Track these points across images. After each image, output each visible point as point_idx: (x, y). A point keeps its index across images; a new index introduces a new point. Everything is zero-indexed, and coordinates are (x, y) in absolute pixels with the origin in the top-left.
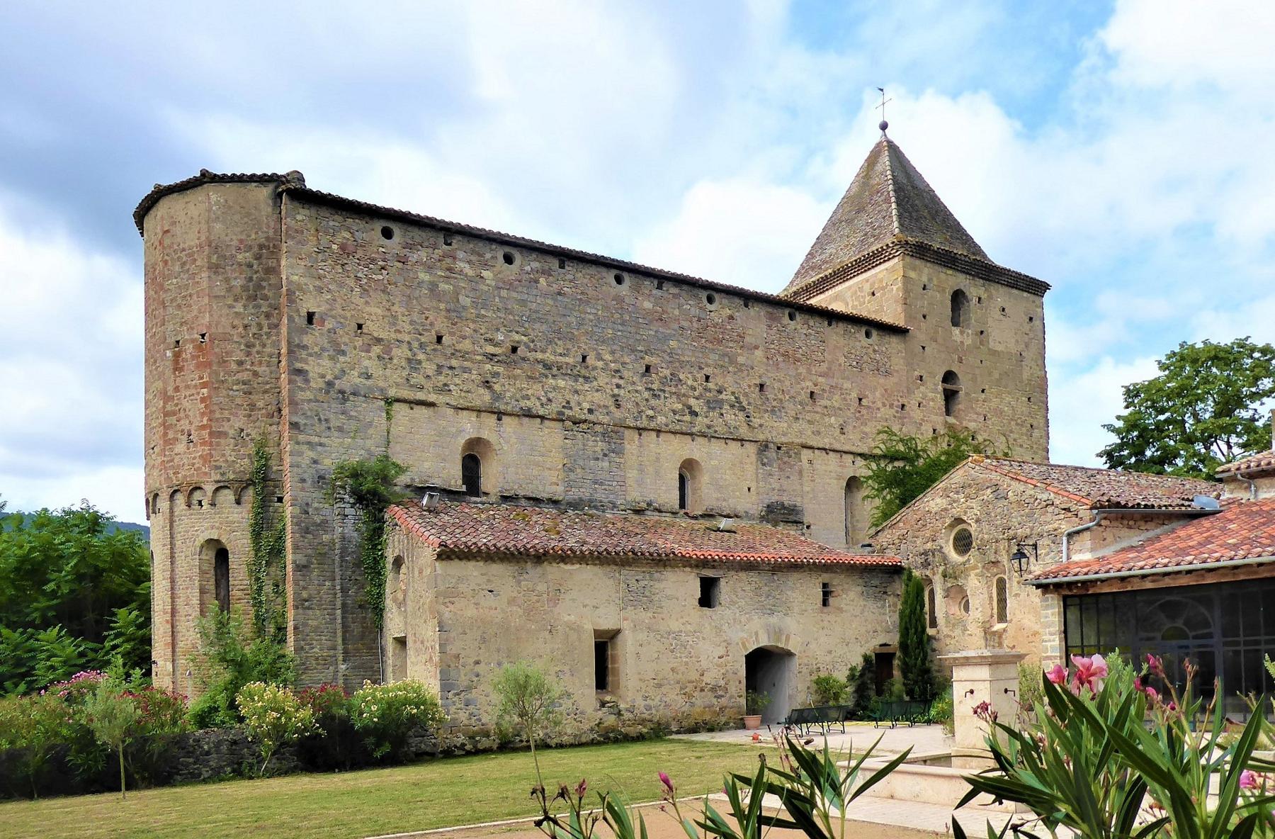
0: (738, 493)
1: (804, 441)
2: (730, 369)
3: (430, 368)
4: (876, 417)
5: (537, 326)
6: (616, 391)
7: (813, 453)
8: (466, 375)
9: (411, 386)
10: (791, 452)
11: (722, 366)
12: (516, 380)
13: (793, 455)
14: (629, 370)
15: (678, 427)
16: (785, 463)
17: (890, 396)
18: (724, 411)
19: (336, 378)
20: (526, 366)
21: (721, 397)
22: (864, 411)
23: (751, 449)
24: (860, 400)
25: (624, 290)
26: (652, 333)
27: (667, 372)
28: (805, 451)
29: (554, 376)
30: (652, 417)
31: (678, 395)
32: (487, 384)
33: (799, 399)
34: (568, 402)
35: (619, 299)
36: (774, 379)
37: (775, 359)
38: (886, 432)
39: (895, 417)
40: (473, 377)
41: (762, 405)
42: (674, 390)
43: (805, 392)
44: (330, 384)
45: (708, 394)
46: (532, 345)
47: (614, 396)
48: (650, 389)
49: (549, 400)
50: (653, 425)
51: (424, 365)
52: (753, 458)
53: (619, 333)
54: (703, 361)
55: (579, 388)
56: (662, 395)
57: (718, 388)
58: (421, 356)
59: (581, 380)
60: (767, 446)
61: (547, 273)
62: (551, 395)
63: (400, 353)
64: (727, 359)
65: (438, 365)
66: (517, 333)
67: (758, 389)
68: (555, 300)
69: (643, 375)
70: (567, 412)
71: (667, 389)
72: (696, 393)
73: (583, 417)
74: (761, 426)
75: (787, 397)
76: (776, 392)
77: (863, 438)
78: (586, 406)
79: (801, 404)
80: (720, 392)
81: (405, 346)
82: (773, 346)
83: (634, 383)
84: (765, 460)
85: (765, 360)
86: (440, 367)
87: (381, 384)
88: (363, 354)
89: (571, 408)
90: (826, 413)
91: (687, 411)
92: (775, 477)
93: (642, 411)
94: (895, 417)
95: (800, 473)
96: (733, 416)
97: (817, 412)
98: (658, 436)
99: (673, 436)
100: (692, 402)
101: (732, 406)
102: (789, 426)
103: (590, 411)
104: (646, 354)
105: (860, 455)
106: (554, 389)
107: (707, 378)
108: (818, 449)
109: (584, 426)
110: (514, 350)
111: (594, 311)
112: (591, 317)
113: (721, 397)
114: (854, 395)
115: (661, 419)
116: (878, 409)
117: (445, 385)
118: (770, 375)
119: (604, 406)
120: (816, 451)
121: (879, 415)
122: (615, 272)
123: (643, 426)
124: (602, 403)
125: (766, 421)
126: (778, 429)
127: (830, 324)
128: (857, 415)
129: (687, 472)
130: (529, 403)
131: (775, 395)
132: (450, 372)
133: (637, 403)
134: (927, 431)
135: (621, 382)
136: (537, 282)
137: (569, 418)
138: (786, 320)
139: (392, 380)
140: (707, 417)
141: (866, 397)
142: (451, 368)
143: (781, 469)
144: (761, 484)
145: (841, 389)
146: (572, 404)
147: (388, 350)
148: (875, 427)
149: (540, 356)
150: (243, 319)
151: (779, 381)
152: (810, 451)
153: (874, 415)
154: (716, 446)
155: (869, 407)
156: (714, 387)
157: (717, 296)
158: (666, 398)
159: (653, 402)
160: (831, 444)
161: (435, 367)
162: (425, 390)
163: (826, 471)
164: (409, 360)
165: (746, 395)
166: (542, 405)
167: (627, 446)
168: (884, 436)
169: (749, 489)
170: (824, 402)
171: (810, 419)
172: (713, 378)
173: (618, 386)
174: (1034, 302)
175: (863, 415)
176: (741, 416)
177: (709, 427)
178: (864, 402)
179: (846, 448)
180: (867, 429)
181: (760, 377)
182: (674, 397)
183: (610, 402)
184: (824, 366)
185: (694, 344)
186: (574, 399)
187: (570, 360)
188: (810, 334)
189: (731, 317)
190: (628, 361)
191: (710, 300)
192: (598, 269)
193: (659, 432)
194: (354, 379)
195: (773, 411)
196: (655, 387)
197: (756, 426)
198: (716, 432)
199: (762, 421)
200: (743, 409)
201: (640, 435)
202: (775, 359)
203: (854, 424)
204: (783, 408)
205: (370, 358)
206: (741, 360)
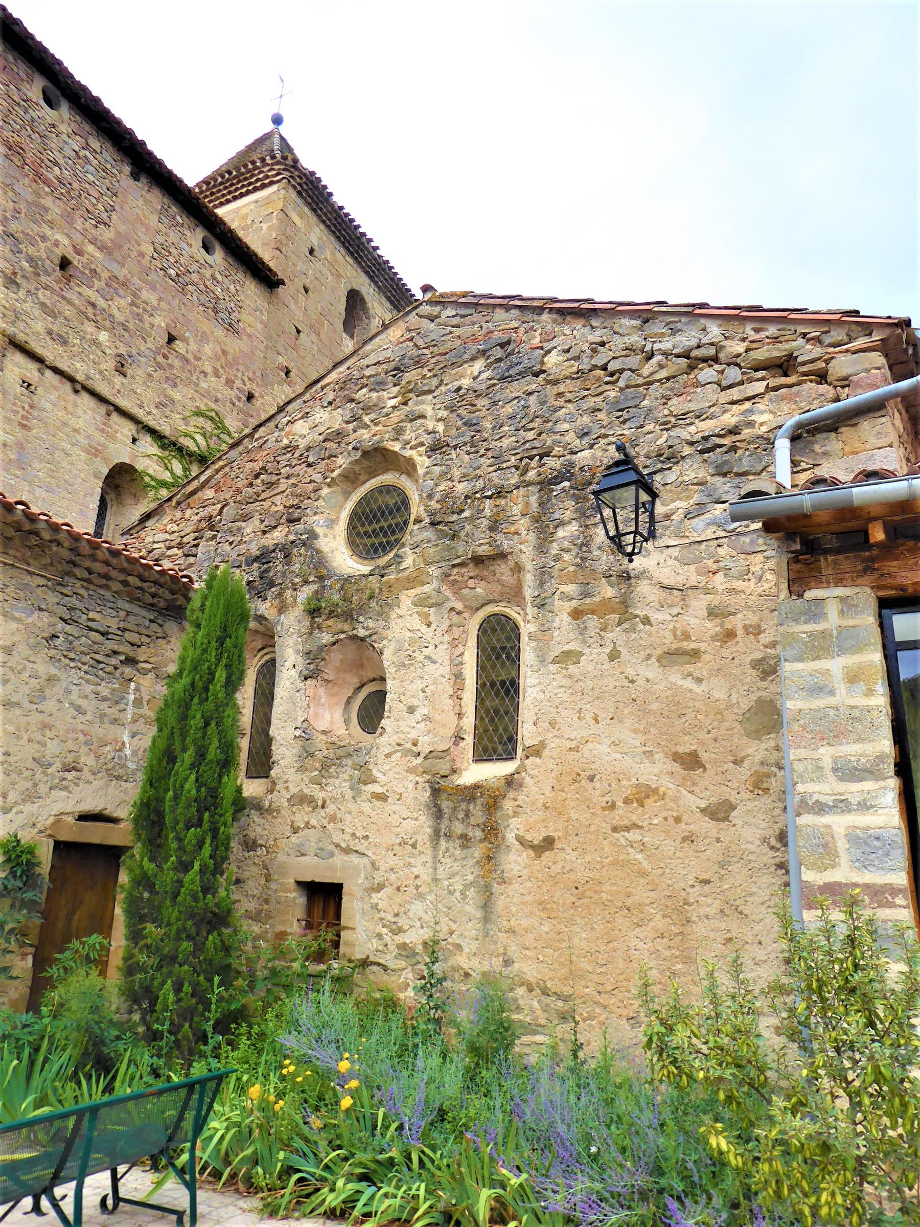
1: (21, 337)
4: (197, 385)
17: (229, 365)
24: (171, 339)
38: (211, 419)
79: (31, 260)
97: (70, 303)
105: (152, 432)
108: (56, 370)
114: (160, 321)
116: (205, 374)
120: (48, 373)
121: (203, 385)
128: (160, 359)
141: (185, 340)
145: (135, 295)
152: (33, 366)
153: (194, 379)
160: (88, 377)
163: (65, 424)
168: (209, 426)
171: (48, 302)
175: (171, 366)
180: (176, 395)
184: (106, 235)
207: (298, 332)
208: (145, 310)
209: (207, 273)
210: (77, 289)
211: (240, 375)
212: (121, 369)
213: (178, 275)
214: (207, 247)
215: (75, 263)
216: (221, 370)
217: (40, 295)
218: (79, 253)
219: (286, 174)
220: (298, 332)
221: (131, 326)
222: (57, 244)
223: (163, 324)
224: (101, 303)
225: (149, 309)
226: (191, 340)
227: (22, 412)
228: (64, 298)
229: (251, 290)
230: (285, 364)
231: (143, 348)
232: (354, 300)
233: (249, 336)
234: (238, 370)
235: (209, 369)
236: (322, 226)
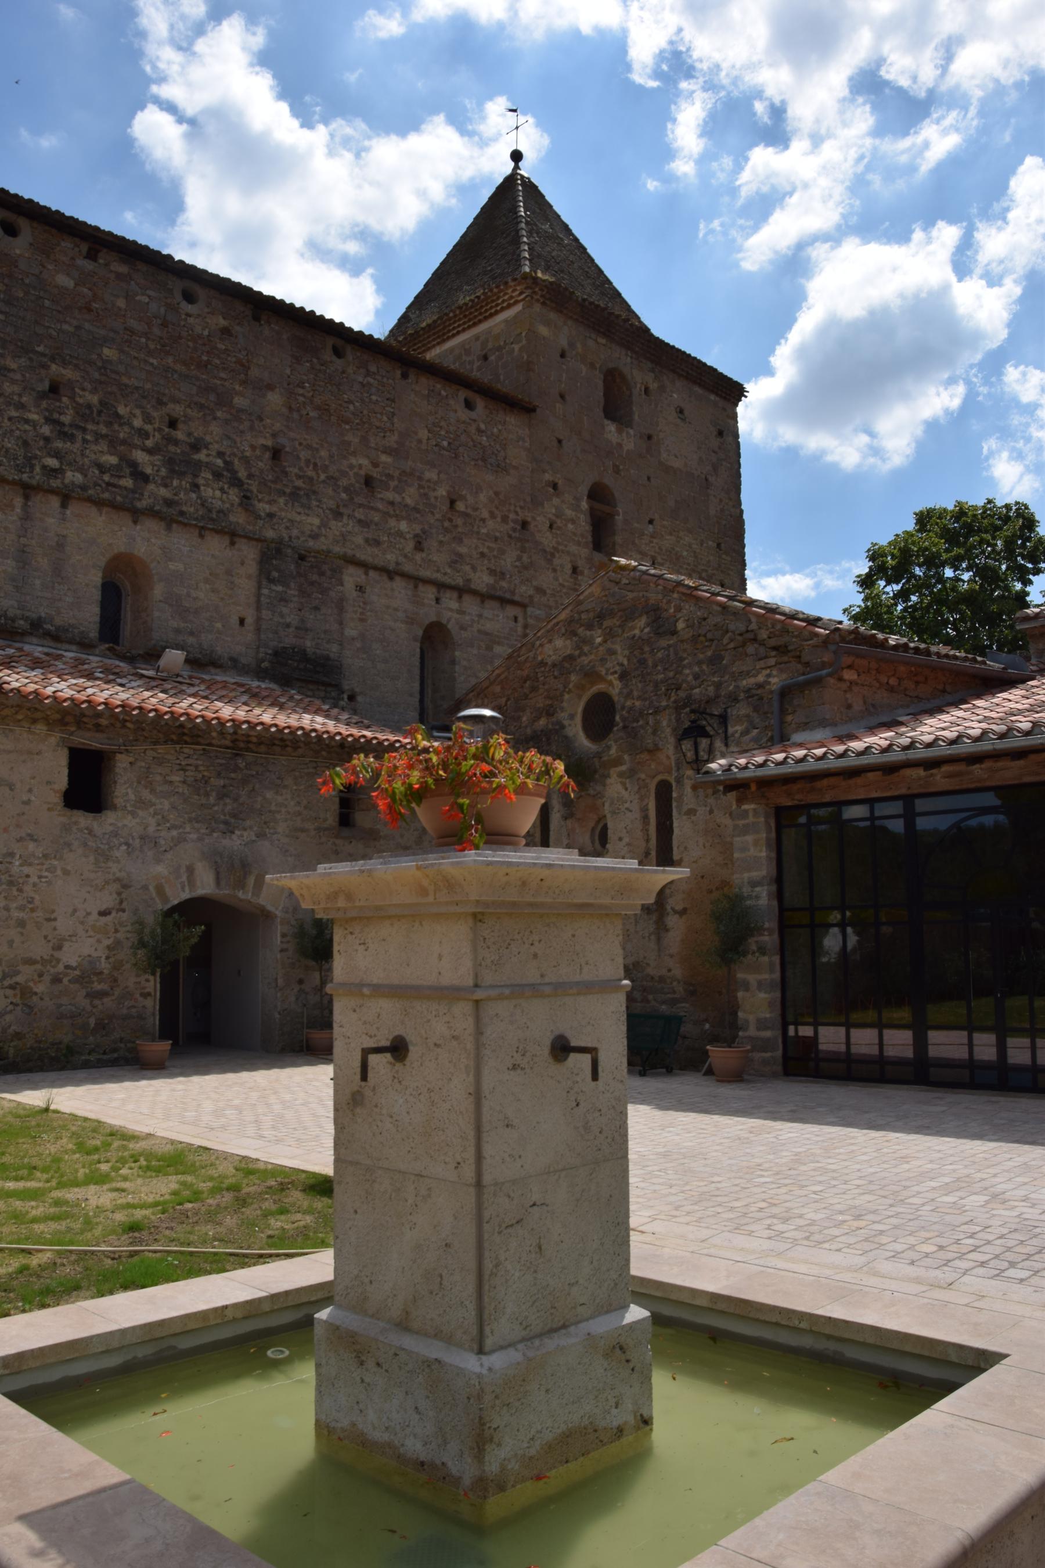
0: (219, 625)
1: (350, 552)
2: (219, 414)
4: (478, 533)
7: (366, 574)
10: (325, 567)
11: (202, 407)
13: (329, 573)
14: (13, 382)
15: (106, 495)
16: (312, 583)
18: (201, 481)
21: (196, 457)
22: (459, 521)
23: (250, 553)
24: (452, 502)
27: (94, 399)
28: (351, 570)
31: (113, 443)
33: (344, 482)
36: (300, 444)
37: (304, 412)
39: (510, 536)
41: (274, 482)
42: (104, 430)
43: (356, 474)
45: (172, 448)
48: (57, 422)
50: (55, 483)
52: (252, 568)
54: (167, 391)
56: (79, 436)
60: (279, 551)
64: (212, 397)
67: (268, 455)
69: (42, 396)
72: (149, 443)
74: (271, 515)
75: (323, 477)
76: (302, 464)
77: (455, 562)
79: (346, 490)
80: (196, 447)
82: (301, 391)
83: (21, 406)
84: (275, 574)
85: (285, 410)
90: (392, 512)
91: (128, 471)
92: (292, 605)
93: (36, 457)
94: (510, 536)
95: (340, 605)
96: (218, 493)
97: (377, 510)
98: (64, 505)
99: (93, 511)
100: (140, 456)
101: (217, 475)
102: (324, 525)
104: (53, 359)
107: (173, 424)
108: (376, 568)
113: (196, 457)
114: (442, 492)
115: (73, 477)
116: (483, 520)
118: (292, 434)
120: (371, 573)
121: (484, 531)
123: (34, 482)
125: (281, 510)
127: (405, 376)
128: (446, 524)
131: (301, 469)
133: (26, 443)
134: (562, 566)
138: (328, 355)
140: (166, 486)
141: (463, 498)
144: (265, 614)
145: (420, 478)
148: (476, 547)
151: (309, 447)
153: (475, 529)
154: (181, 541)
155: (467, 515)
156: (186, 439)
157: (201, 293)
158: (85, 441)
159: (59, 444)
160: (397, 564)
163: (388, 607)
165: (246, 460)
169: (242, 621)
170: (390, 495)
171: (362, 517)
172: (185, 422)
174: (724, 409)
175: (456, 526)
176: (234, 495)
177: (169, 503)
178: (460, 506)
179: (426, 573)
180: (463, 550)
181: (274, 436)
182: (103, 446)
185: (151, 360)
188: (369, 383)
189: (226, 331)
191: (189, 297)
193: (66, 498)
195: (294, 496)
196: (66, 419)
197: (263, 514)
198: (182, 513)
199: (274, 509)
200: (237, 483)
201: (27, 497)
202: (304, 412)
203: (441, 537)
204: (314, 492)
206: (238, 401)
207: (560, 441)
208: (429, 487)
209: (472, 429)
210: (379, 496)
211: (512, 508)
212: (419, 547)
213: (449, 444)
214: (469, 405)
215: (375, 475)
216: (496, 512)
217: (357, 515)
218: (375, 465)
219: (528, 292)
220: (560, 441)
221: (421, 507)
222: (360, 466)
223: (444, 493)
224: (398, 498)
225: (432, 485)
226: (468, 496)
227: (360, 610)
228: (372, 508)
229: (513, 424)
230: (551, 479)
231: (432, 521)
232: (613, 380)
233: (516, 468)
234: (510, 504)
235: (485, 514)
236: (570, 323)
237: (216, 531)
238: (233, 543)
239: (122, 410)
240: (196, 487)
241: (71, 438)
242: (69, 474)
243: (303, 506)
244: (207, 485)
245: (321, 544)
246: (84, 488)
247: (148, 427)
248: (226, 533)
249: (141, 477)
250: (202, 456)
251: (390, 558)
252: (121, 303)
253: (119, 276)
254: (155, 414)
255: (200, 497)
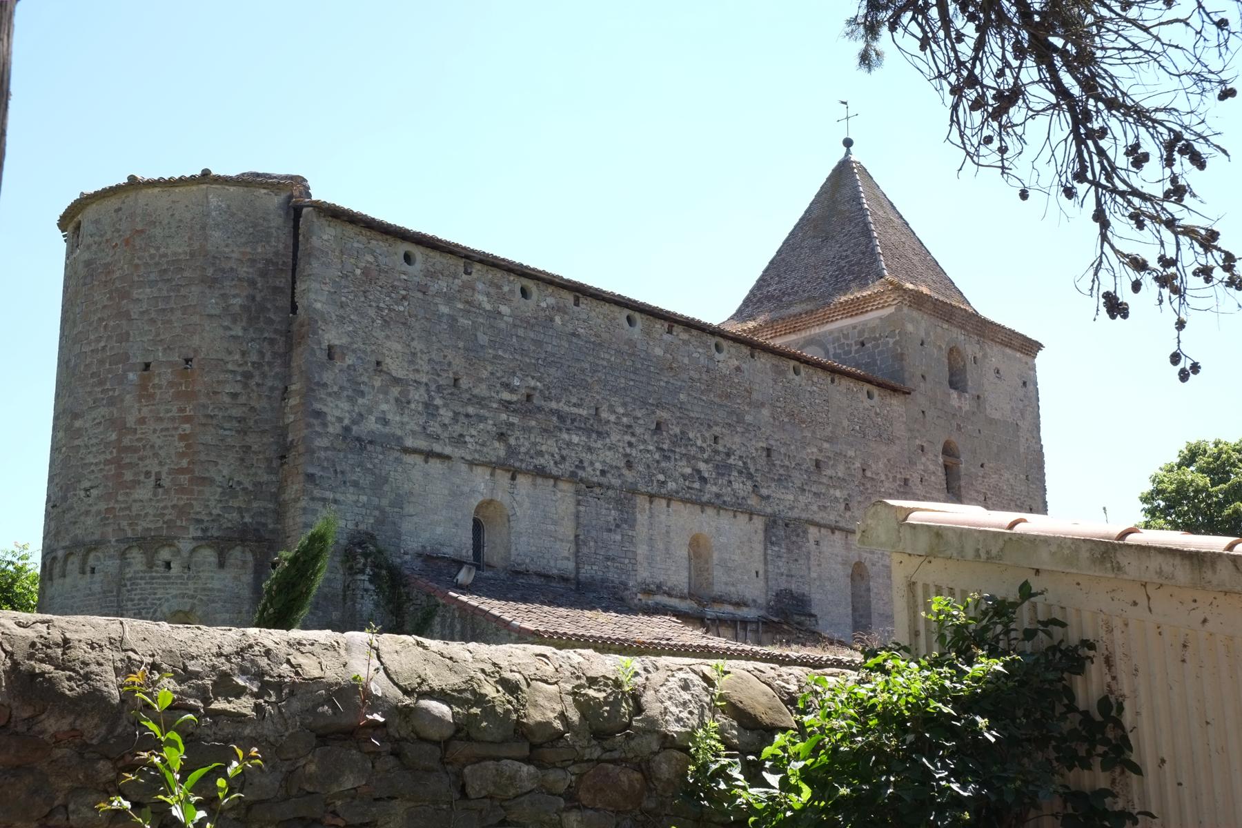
1: (811, 517)
3: (446, 415)
5: (552, 371)
6: (628, 450)
8: (481, 426)
9: (429, 436)
12: (530, 432)
15: (688, 496)
18: (732, 478)
19: (354, 422)
20: (539, 416)
23: (759, 523)
25: (636, 332)
26: (662, 384)
27: (677, 430)
29: (568, 430)
30: (663, 482)
31: (689, 458)
32: (502, 436)
34: (581, 461)
35: (631, 343)
40: (489, 428)
41: (769, 472)
44: (347, 429)
45: (717, 458)
46: (547, 392)
47: (626, 455)
48: (662, 450)
49: (563, 458)
50: (663, 491)
51: (442, 411)
53: (632, 383)
55: (593, 445)
56: (672, 455)
57: (726, 451)
58: (438, 402)
59: (594, 436)
61: (561, 310)
62: (564, 452)
63: (417, 395)
65: (454, 412)
66: (533, 378)
68: (570, 342)
70: (581, 473)
71: (677, 450)
72: (706, 456)
73: (595, 479)
78: (598, 466)
80: (728, 455)
81: (422, 390)
83: (645, 442)
86: (456, 414)
87: (399, 433)
88: (381, 396)
89: (584, 468)
91: (697, 477)
93: (654, 475)
101: (740, 472)
102: (796, 500)
103: (603, 473)
106: (568, 445)
107: (716, 438)
109: (597, 490)
110: (529, 397)
111: (607, 356)
112: (605, 363)
115: (672, 485)
117: (461, 435)
119: (616, 467)
122: (627, 312)
123: (653, 492)
124: (614, 464)
126: (786, 500)
129: (697, 548)
130: (542, 461)
132: (466, 421)
135: (633, 440)
136: (552, 320)
137: (581, 480)
139: (406, 426)
140: (715, 484)
142: (467, 416)
143: (789, 551)
146: (586, 464)
147: (404, 393)
149: (554, 405)
150: (241, 344)
154: (725, 520)
159: (663, 464)
160: (836, 522)
161: (451, 414)
162: (441, 442)
164: (427, 405)
166: (556, 463)
167: (639, 516)
173: (630, 444)
177: (718, 496)
182: (684, 463)
183: (622, 464)
186: (587, 457)
187: (584, 413)
190: (640, 415)
192: (612, 309)
193: (669, 499)
194: (371, 424)
196: (665, 447)
198: (724, 502)
200: (750, 476)
201: (651, 502)
205: (387, 402)
206: (748, 418)
237: (742, 512)
238: (751, 519)
239: (691, 435)
240: (730, 482)
241: (667, 458)
242: (670, 484)
243: (785, 488)
244: (735, 481)
245: (795, 514)
246: (677, 492)
247: (704, 445)
248: (746, 513)
249: (703, 480)
250: (731, 461)
251: (831, 517)
252: (686, 361)
253: (684, 341)
254: (707, 435)
255: (732, 490)
